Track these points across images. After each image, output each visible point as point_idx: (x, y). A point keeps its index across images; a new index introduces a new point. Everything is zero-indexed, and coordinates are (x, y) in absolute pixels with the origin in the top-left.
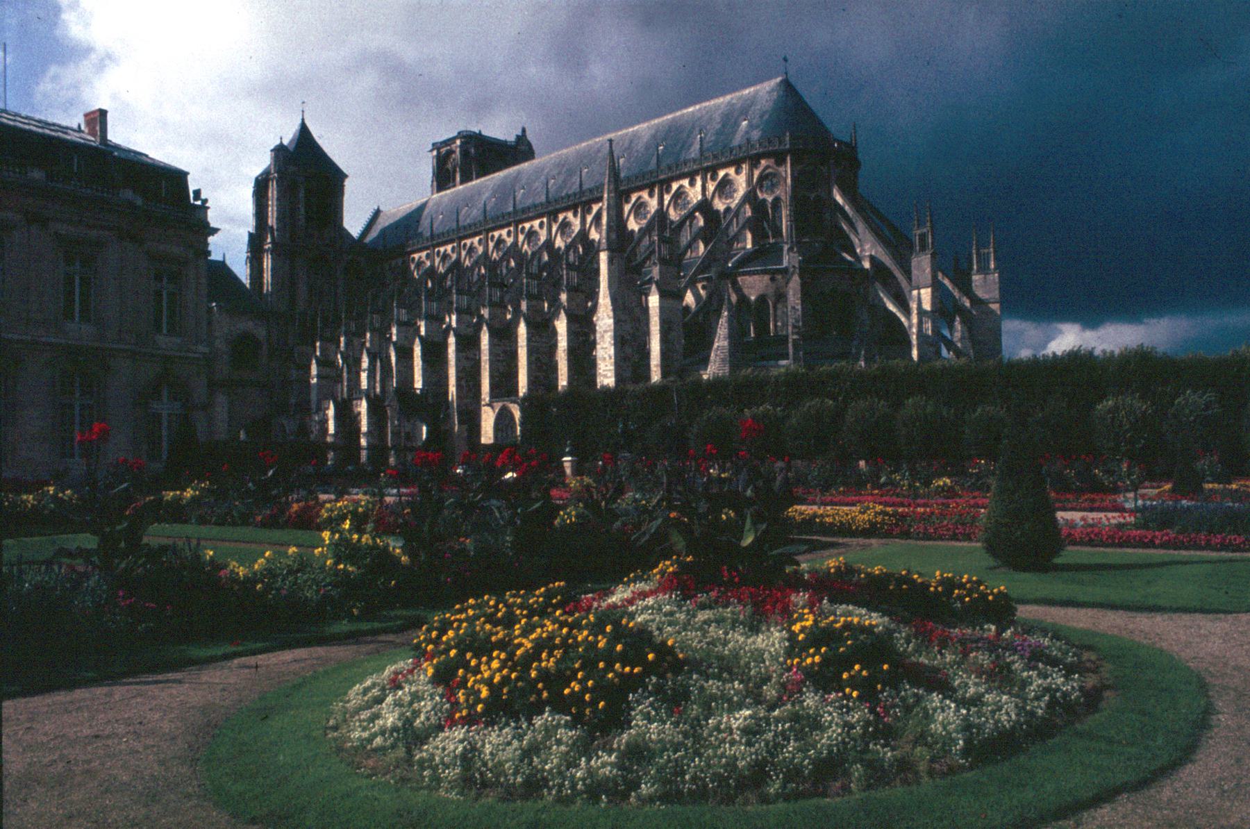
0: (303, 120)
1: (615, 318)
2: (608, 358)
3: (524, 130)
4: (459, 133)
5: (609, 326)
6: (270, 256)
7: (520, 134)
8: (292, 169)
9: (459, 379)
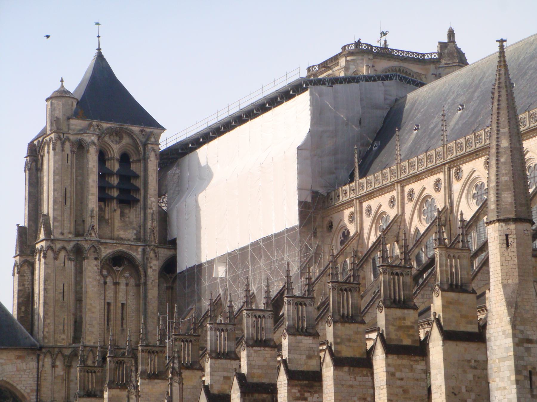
0: (99, 49)
1: (514, 336)
3: (451, 33)
4: (344, 48)
5: (507, 349)
6: (43, 260)
7: (446, 40)
8: (77, 124)
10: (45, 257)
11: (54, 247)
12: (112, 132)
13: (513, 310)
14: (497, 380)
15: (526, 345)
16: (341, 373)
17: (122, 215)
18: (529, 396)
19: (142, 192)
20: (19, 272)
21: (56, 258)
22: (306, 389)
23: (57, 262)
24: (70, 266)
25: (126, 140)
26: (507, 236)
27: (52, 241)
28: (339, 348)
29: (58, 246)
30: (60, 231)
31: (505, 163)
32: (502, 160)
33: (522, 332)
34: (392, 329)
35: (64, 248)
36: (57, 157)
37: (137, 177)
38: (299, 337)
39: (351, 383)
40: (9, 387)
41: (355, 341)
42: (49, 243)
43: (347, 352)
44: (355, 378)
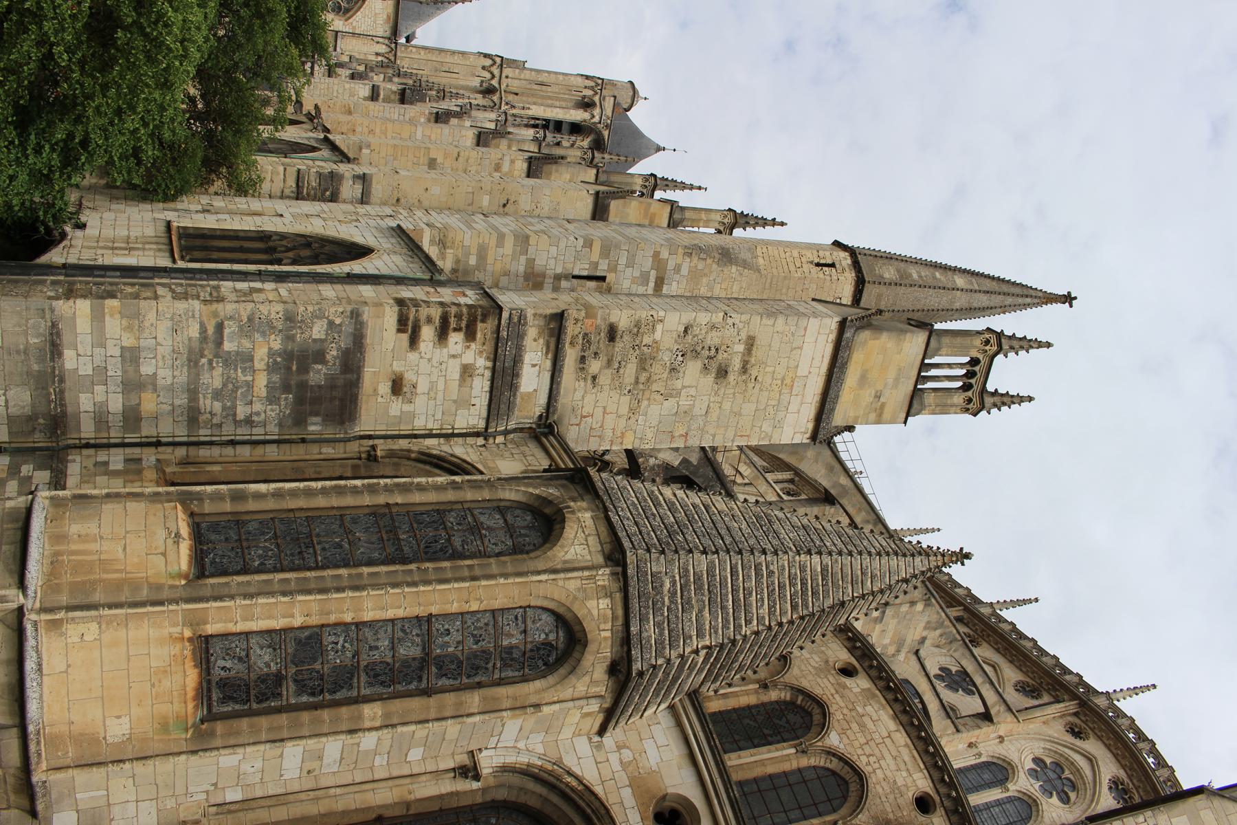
0: (664, 149)
11: (495, 67)
15: (653, 273)
18: (559, 270)
21: (484, 68)
24: (476, 82)
26: (832, 265)
27: (501, 65)
29: (496, 72)
33: (677, 269)
35: (493, 76)
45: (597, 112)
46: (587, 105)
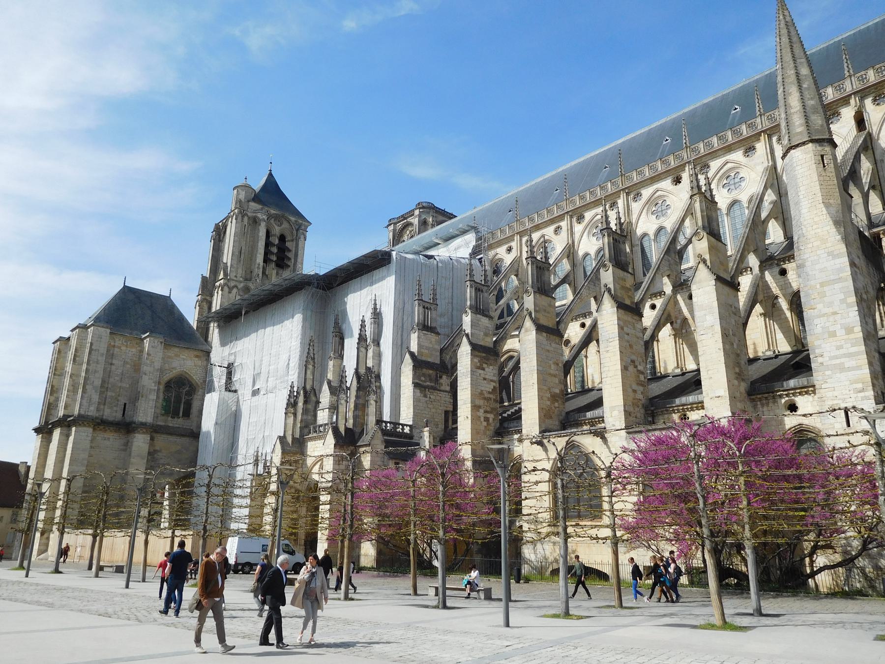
0: (271, 170)
2: (841, 333)
6: (220, 292)
8: (254, 206)
9: (475, 407)
10: (222, 290)
12: (277, 218)
13: (842, 229)
14: (820, 306)
16: (541, 338)
17: (277, 274)
19: (293, 260)
20: (199, 306)
21: (230, 292)
22: (484, 360)
23: (231, 295)
25: (285, 225)
26: (822, 156)
28: (538, 315)
29: (232, 284)
30: (235, 275)
31: (808, 89)
32: (805, 86)
34: (618, 287)
35: (236, 286)
36: (238, 225)
37: (289, 251)
38: (479, 316)
39: (548, 348)
40: (187, 376)
41: (548, 313)
42: (226, 281)
43: (543, 321)
44: (550, 344)
45: (259, 215)
46: (255, 221)
